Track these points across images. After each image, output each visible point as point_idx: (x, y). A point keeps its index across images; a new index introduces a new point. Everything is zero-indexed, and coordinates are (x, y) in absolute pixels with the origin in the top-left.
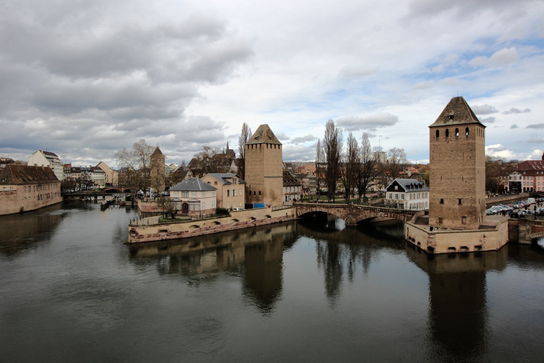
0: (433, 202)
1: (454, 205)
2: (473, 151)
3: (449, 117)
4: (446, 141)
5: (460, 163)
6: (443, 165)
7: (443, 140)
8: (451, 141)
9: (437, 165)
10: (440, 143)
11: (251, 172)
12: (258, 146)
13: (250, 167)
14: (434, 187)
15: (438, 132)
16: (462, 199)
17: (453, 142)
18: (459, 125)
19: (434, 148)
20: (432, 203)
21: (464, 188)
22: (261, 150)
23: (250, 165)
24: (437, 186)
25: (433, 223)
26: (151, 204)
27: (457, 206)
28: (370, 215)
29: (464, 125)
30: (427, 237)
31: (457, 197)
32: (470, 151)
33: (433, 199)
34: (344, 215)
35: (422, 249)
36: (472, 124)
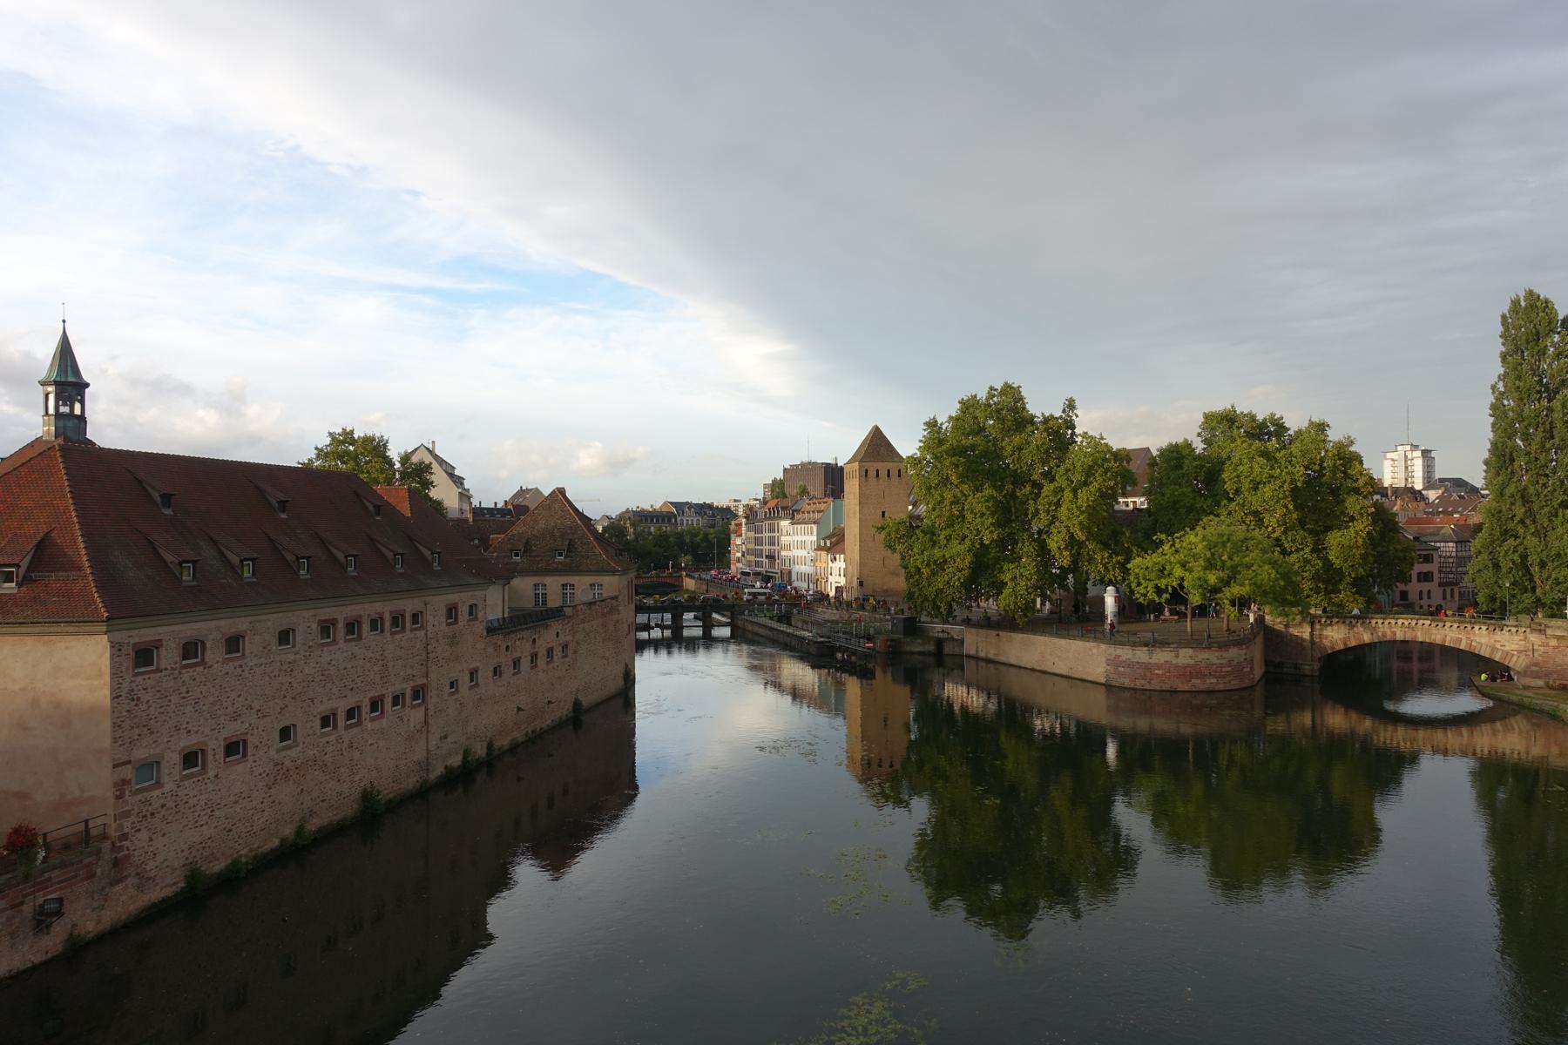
26: (1177, 656)
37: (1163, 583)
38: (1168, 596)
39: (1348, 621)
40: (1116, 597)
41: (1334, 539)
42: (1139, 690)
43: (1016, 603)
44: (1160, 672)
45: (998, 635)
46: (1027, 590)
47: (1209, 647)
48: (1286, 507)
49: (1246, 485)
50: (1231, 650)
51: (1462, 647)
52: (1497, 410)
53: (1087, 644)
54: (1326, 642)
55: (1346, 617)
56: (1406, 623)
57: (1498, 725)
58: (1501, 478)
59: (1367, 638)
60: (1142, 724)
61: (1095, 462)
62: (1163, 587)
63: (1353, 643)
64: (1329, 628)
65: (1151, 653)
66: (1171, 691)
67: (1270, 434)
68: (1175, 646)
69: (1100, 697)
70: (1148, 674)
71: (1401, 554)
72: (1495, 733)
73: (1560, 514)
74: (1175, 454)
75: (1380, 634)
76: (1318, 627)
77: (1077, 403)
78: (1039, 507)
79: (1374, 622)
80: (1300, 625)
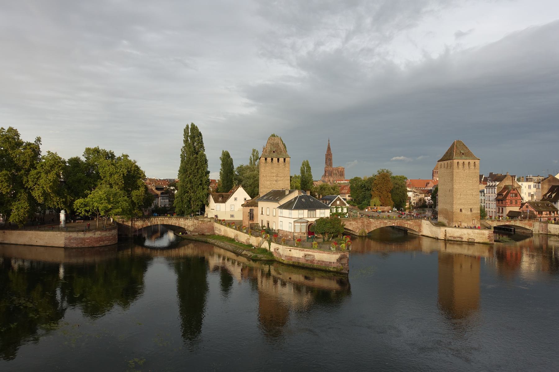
0: (456, 211)
5: (471, 185)
7: (462, 169)
8: (466, 170)
9: (458, 185)
11: (270, 188)
12: (281, 160)
13: (268, 183)
14: (456, 201)
17: (467, 171)
20: (455, 212)
21: (473, 201)
22: (285, 165)
23: (268, 181)
24: (458, 200)
26: (95, 234)
27: (469, 213)
30: (488, 233)
32: (476, 177)
33: (456, 209)
34: (356, 227)
35: (479, 243)
37: (88, 208)
38: (91, 213)
39: (143, 219)
40: (65, 214)
41: (134, 193)
42: (79, 248)
43: (19, 219)
44: (88, 241)
45: (4, 232)
46: (24, 213)
47: (106, 230)
48: (122, 182)
49: (108, 174)
50: (112, 231)
51: (177, 225)
52: (182, 156)
53: (55, 233)
54: (136, 227)
55: (143, 218)
56: (161, 219)
57: (186, 247)
58: (183, 176)
59: (149, 224)
60: (74, 261)
61: (55, 162)
62: (88, 210)
63: (145, 226)
64: (137, 222)
65: (85, 234)
66: (93, 247)
67: (109, 157)
68: (94, 231)
69: (62, 253)
70: (83, 242)
71: (151, 198)
72: (185, 249)
73: (199, 187)
74: (76, 162)
75: (153, 223)
76: (133, 222)
77: (41, 140)
78: (29, 179)
79: (152, 219)
80: (127, 221)
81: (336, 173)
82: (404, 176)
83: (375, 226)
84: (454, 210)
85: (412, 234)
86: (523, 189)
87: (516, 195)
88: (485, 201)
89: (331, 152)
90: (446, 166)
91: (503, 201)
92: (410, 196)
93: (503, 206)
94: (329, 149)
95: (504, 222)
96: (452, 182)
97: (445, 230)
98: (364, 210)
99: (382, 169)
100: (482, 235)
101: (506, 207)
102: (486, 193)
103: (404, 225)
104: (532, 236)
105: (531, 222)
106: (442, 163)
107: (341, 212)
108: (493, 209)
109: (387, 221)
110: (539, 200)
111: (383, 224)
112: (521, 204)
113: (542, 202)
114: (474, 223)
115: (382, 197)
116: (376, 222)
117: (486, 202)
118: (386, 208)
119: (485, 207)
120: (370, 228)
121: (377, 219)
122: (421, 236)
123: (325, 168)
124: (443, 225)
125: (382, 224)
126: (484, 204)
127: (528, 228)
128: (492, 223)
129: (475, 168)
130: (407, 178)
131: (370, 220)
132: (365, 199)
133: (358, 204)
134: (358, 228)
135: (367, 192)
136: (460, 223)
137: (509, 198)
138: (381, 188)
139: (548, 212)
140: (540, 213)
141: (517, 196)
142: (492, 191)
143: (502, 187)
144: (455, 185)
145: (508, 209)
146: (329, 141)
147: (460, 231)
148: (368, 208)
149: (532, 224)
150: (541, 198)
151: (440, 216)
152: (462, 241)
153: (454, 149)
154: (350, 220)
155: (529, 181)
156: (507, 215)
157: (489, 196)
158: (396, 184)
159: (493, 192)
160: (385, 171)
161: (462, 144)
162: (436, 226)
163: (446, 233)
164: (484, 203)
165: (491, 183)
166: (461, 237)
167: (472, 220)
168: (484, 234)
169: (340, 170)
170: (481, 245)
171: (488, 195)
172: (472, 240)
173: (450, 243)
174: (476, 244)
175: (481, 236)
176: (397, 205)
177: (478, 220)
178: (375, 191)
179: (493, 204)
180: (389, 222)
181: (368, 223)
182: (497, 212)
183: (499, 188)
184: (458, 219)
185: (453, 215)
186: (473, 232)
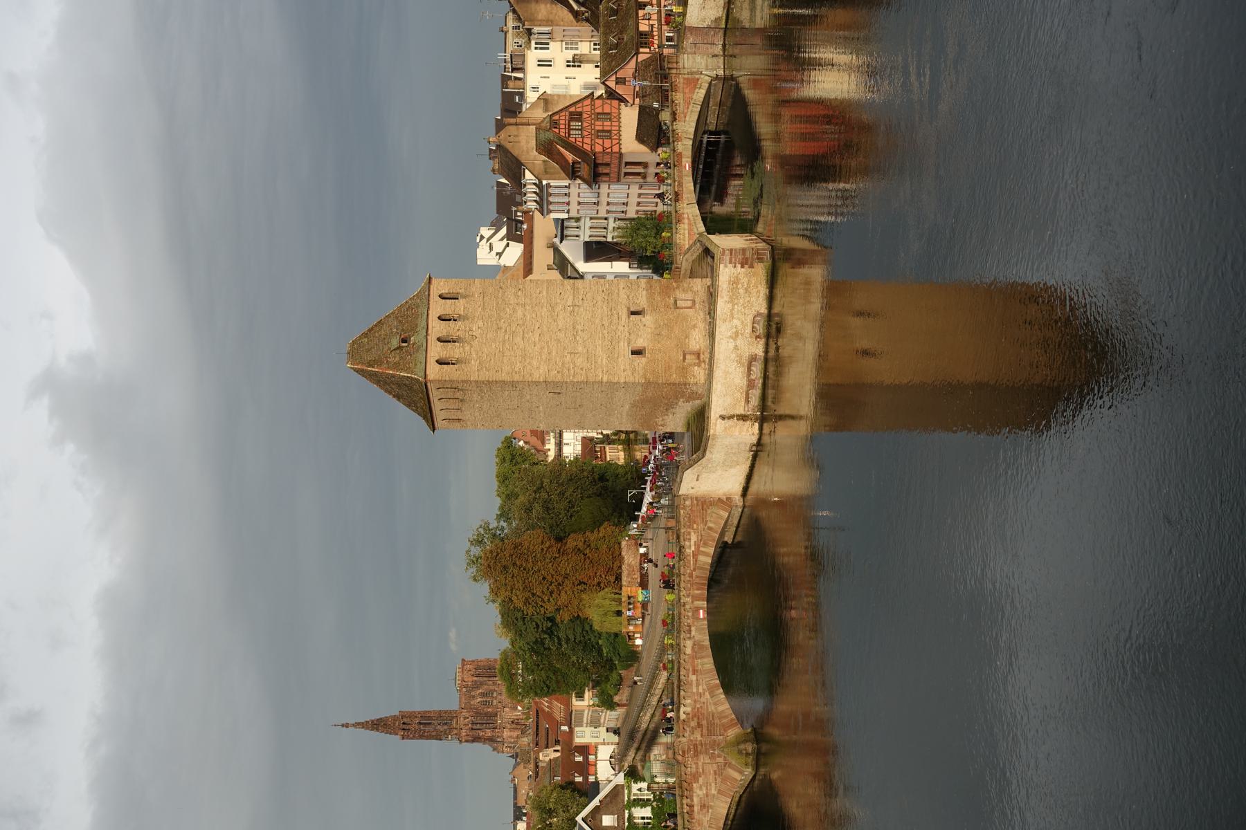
0: (641, 373)
1: (645, 325)
2: (501, 284)
3: (406, 344)
4: (472, 343)
6: (536, 348)
9: (535, 363)
10: (474, 355)
15: (440, 362)
16: (628, 308)
17: (476, 327)
18: (430, 312)
19: (488, 371)
20: (644, 376)
25: (702, 374)
27: (648, 319)
28: (709, 671)
29: (431, 302)
31: (624, 319)
32: (501, 291)
34: (719, 780)
35: (771, 299)
36: (431, 286)
81: (483, 695)
82: (499, 450)
83: (712, 697)
84: (638, 378)
85: (740, 529)
86: (554, 86)
87: (577, 116)
88: (599, 215)
89: (395, 718)
90: (452, 405)
91: (599, 161)
92: (579, 438)
93: (617, 161)
94: (379, 725)
95: (681, 177)
96: (520, 387)
97: (720, 421)
98: (640, 648)
99: (468, 564)
100: (740, 286)
101: (621, 155)
102: (568, 212)
103: (702, 568)
104: (732, 78)
105: (680, 81)
106: (439, 416)
107: (649, 809)
108: (630, 191)
109: (689, 644)
110: (595, 33)
111: (699, 661)
112: (609, 102)
113: (601, 29)
114: (689, 304)
115: (582, 576)
116: (695, 690)
117: (602, 214)
118: (630, 558)
119: (623, 216)
120: (721, 716)
121: (679, 687)
122: (749, 497)
123: (461, 741)
124: (700, 418)
125: (702, 664)
126: (611, 221)
127: (703, 92)
128: (686, 221)
129: (465, 297)
130: (507, 438)
131: (683, 716)
132: (590, 639)
133: (612, 668)
134: (719, 772)
135: (561, 634)
136: (688, 357)
137: (587, 141)
138: (544, 578)
139: (641, 13)
140: (643, 39)
141: (580, 114)
142: (558, 195)
143: (544, 161)
144: (531, 375)
145: (630, 144)
146: (346, 725)
147: (723, 367)
148: (628, 633)
149: (688, 79)
150: (587, 28)
151: (662, 425)
152: (766, 360)
153: (382, 373)
154: (686, 809)
155: (523, 62)
156: (654, 148)
157: (579, 203)
158: (529, 510)
159: (566, 191)
160: (476, 551)
161: (366, 340)
162: (705, 450)
163: (731, 417)
164: (606, 219)
165: (528, 195)
166: (746, 364)
167: (677, 307)
168: (735, 282)
169: (470, 680)
170: (779, 293)
171: (574, 208)
172: (761, 324)
173: (776, 400)
174: (776, 310)
175: (741, 291)
176: (614, 511)
177: (678, 287)
178: (559, 603)
179: (610, 191)
180: (693, 633)
181: (699, 725)
182: (642, 181)
183: (546, 172)
184: (674, 366)
185: (659, 384)
186: (725, 321)
